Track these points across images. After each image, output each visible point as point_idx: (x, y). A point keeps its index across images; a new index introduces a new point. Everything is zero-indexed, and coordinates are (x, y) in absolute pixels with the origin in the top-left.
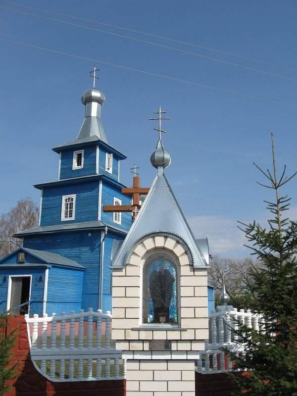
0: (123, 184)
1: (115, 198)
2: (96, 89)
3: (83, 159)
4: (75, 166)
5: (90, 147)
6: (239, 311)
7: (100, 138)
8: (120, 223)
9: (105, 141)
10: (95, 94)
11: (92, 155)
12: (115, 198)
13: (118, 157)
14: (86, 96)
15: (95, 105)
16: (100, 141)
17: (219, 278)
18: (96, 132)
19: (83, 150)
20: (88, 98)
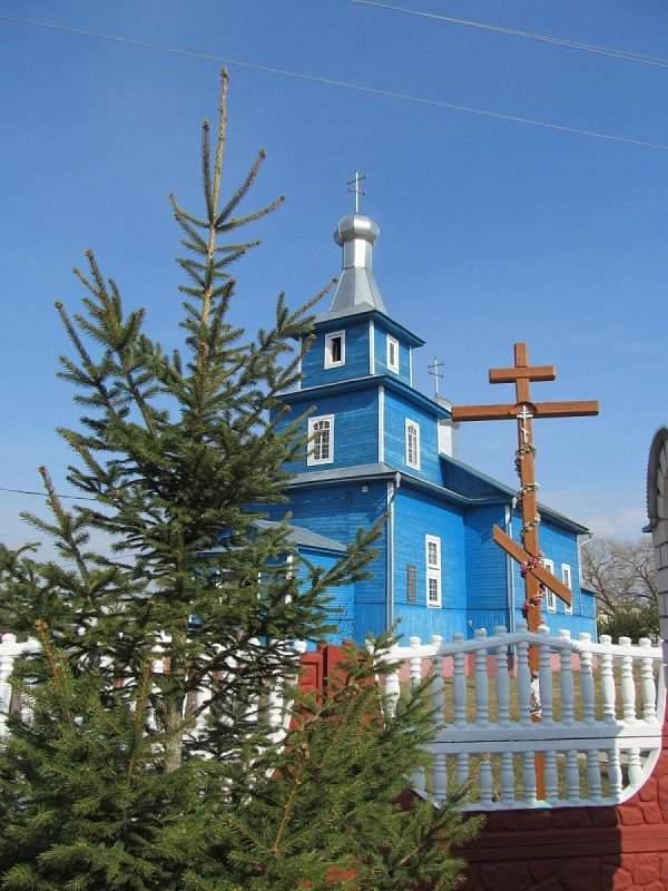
0: (423, 393)
1: (407, 420)
2: (363, 213)
3: (343, 347)
4: (329, 362)
5: (356, 324)
6: (615, 642)
7: (372, 304)
8: (418, 467)
9: (382, 309)
10: (361, 224)
11: (361, 339)
12: (407, 420)
13: (408, 341)
14: (345, 229)
15: (361, 248)
16: (375, 311)
17: (591, 575)
18: (366, 297)
19: (344, 332)
20: (346, 232)
